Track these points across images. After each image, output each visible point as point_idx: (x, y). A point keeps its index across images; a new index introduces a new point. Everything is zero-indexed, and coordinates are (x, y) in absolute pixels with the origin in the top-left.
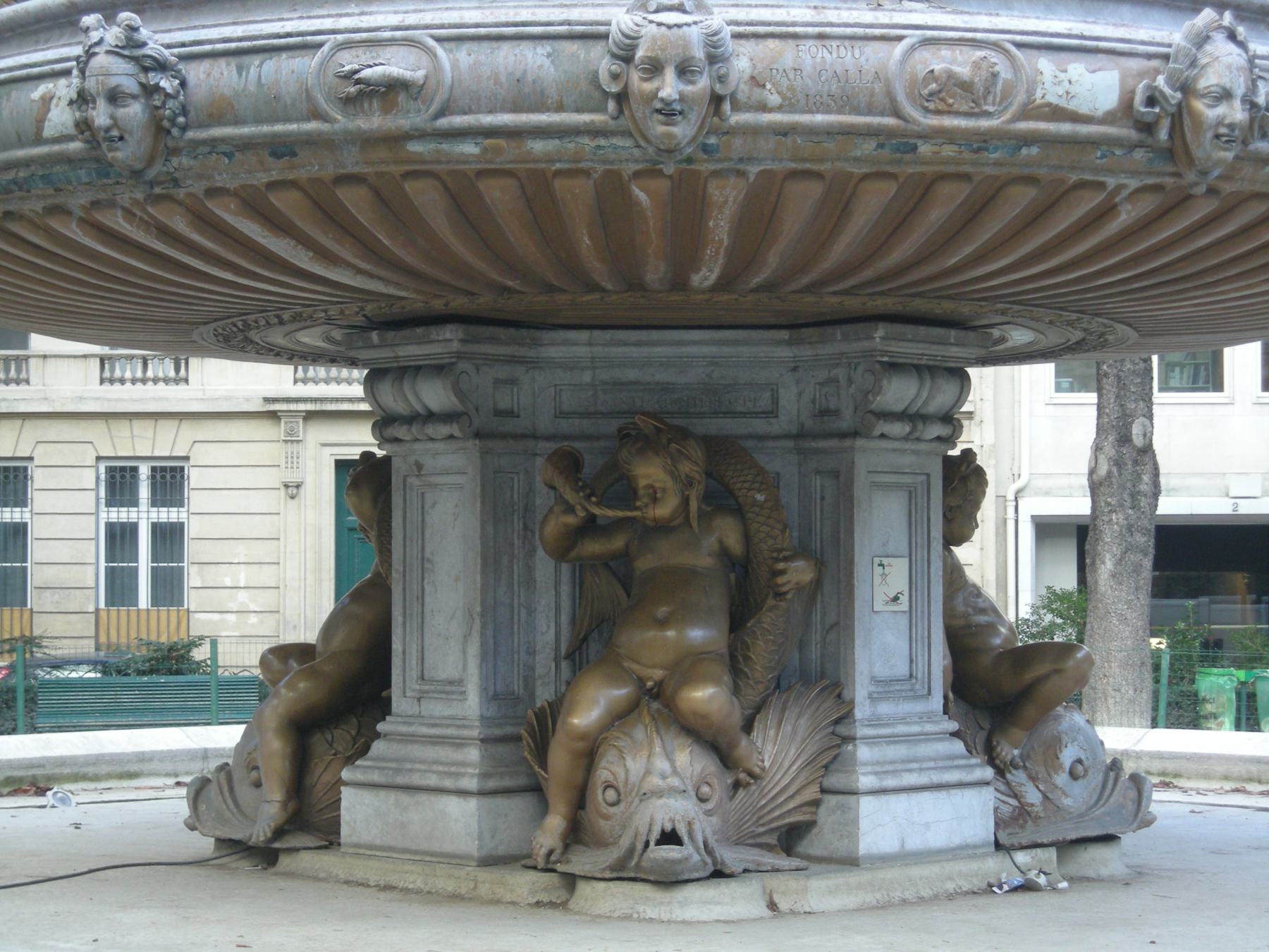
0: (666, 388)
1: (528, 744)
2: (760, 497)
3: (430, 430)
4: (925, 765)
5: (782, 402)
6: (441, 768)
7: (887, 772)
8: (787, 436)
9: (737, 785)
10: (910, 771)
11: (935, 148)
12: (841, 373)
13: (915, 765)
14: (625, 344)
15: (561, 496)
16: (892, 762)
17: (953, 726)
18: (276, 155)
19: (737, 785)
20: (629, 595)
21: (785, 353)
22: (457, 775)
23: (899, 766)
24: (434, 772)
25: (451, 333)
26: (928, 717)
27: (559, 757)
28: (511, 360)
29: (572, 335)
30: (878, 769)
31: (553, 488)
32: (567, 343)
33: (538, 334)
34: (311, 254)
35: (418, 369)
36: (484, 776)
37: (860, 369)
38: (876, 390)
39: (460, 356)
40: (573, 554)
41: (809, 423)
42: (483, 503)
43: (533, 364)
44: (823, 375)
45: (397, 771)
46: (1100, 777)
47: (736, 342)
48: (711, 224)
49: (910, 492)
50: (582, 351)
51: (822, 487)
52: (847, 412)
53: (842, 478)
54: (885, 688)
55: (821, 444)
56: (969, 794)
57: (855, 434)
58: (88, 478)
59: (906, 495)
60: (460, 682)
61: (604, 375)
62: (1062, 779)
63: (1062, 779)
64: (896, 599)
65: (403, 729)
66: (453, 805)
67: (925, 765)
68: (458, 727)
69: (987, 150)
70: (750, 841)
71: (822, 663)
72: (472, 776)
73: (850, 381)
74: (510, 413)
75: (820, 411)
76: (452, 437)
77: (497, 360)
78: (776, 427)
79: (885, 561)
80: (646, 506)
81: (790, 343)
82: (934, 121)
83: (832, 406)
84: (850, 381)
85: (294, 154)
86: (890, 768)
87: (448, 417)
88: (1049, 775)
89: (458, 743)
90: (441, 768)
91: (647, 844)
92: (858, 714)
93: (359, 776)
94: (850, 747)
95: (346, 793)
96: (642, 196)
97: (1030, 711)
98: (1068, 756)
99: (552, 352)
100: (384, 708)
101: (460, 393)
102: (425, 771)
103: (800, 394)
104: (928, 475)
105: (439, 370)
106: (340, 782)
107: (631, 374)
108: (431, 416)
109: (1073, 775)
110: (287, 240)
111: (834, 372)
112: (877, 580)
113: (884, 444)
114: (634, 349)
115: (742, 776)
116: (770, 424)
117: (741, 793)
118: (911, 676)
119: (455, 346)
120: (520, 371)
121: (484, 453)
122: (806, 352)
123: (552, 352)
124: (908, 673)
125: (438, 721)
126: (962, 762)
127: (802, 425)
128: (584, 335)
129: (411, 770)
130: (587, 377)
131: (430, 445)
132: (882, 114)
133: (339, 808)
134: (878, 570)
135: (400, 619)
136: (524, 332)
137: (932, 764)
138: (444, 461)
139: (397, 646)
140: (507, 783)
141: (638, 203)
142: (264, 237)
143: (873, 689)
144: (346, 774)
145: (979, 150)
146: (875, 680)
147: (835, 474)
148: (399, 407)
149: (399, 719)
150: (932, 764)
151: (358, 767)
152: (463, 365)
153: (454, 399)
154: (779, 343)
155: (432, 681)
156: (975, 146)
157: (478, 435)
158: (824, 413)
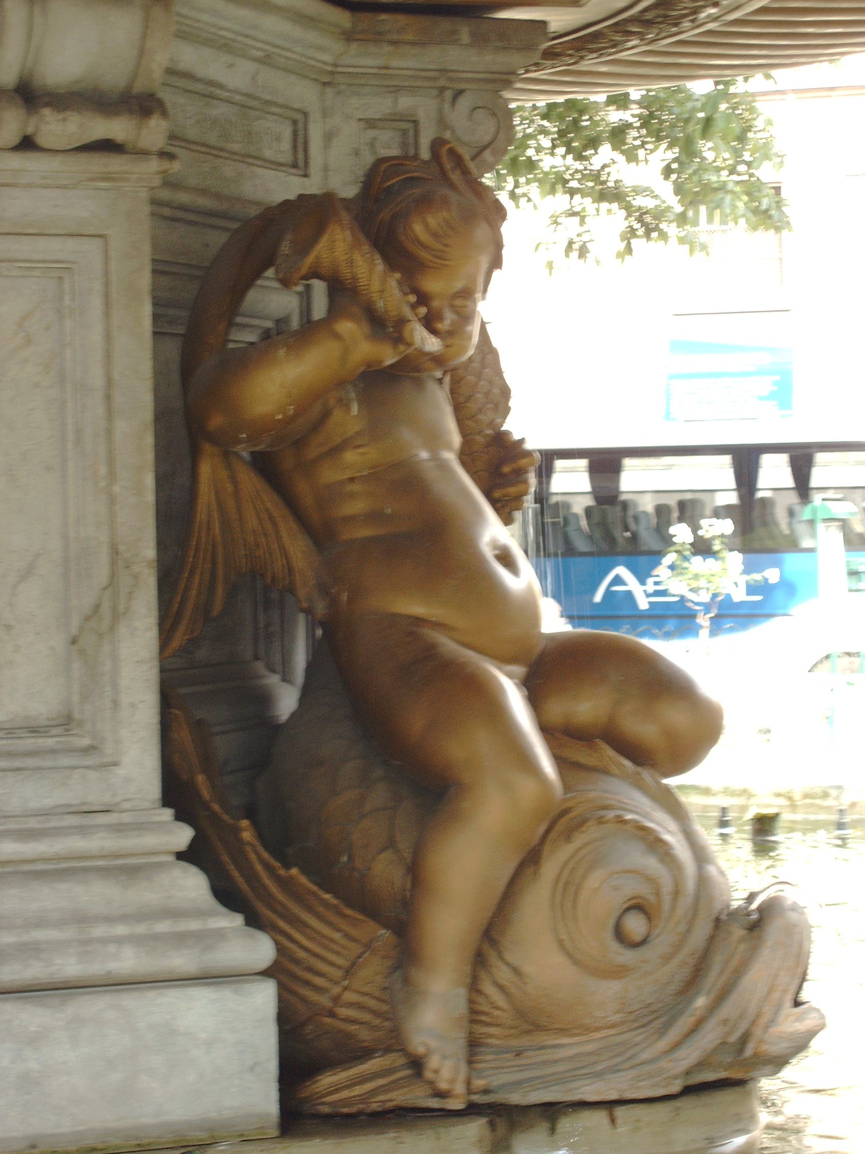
3: (56, 128)
27: (466, 863)
37: (464, 103)
44: (380, 106)
66: (197, 1009)
81: (349, 36)
89: (128, 870)
111: (405, 102)
122: (365, 59)
125: (32, 823)
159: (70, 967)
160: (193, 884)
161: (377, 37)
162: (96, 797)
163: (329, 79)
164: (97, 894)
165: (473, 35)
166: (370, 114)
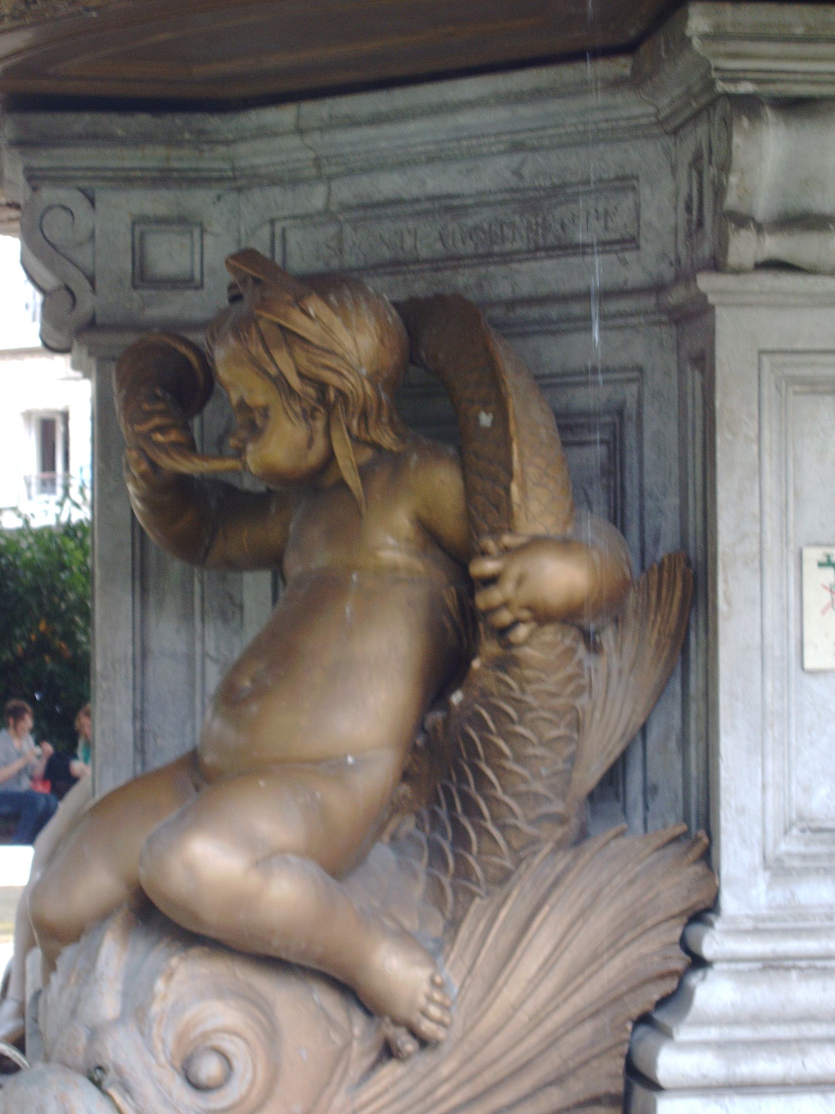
0: (447, 206)
14: (353, 123)
21: (632, 107)
28: (163, 178)
29: (271, 116)
33: (214, 123)
43: (239, 181)
47: (538, 95)
61: (346, 191)
81: (635, 81)
99: (255, 155)
107: (389, 184)
114: (370, 132)
116: (624, 263)
120: (199, 200)
136: (179, 120)
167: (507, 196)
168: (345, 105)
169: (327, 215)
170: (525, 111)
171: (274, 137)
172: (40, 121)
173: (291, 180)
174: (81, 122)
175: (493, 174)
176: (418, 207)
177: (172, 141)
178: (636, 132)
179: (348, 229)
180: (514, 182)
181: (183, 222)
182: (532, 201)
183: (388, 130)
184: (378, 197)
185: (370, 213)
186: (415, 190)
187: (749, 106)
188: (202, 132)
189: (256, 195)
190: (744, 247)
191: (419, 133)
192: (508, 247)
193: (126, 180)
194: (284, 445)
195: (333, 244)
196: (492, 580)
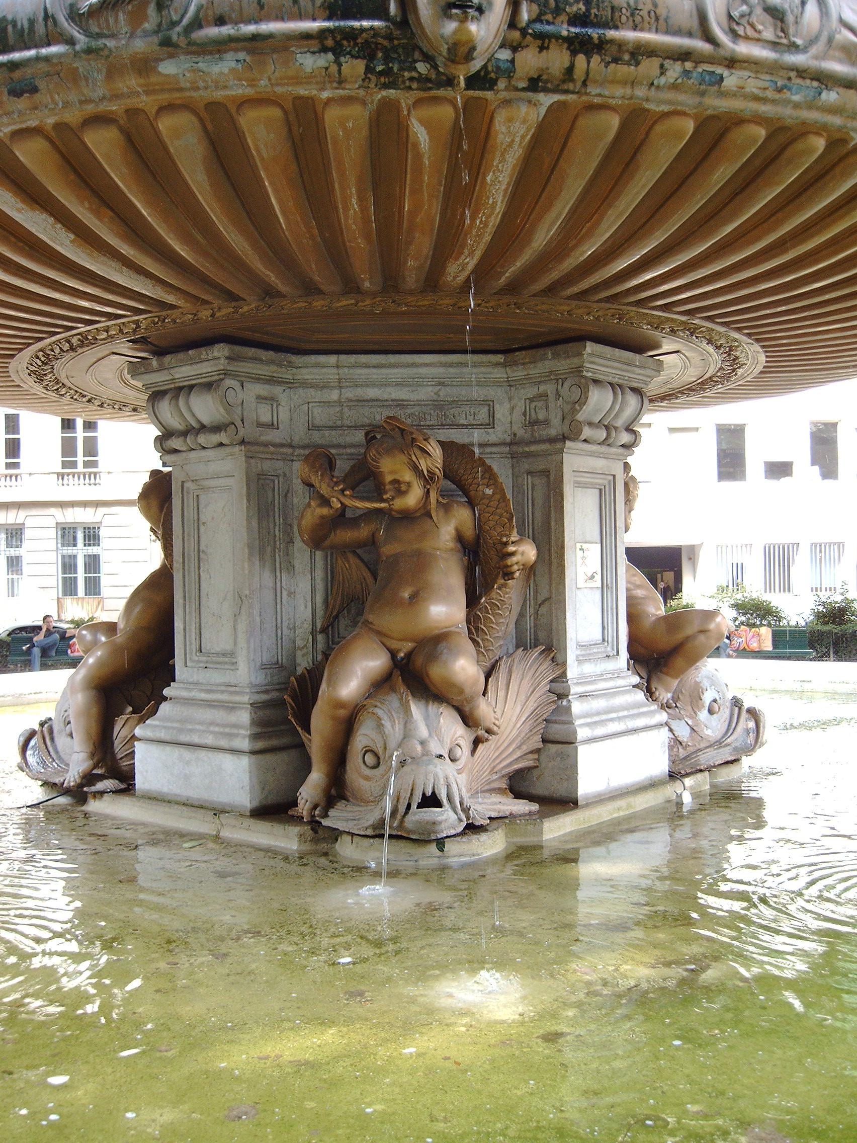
0: (400, 404)
1: (292, 708)
2: (489, 492)
3: (202, 439)
4: (621, 714)
5: (497, 416)
6: (217, 729)
7: (595, 723)
8: (504, 444)
9: (477, 742)
10: (612, 720)
11: (741, 83)
12: (549, 388)
13: (614, 715)
14: (367, 366)
15: (318, 492)
16: (598, 713)
17: (636, 680)
18: (16, 93)
19: (477, 742)
20: (375, 576)
21: (499, 374)
22: (231, 736)
23: (604, 717)
24: (212, 732)
25: (220, 351)
26: (616, 675)
27: (321, 722)
28: (271, 381)
29: (322, 359)
30: (589, 720)
31: (310, 485)
32: (317, 365)
33: (294, 358)
34: (72, 236)
35: (191, 387)
36: (255, 737)
37: (567, 385)
38: (582, 401)
39: (226, 374)
40: (327, 543)
41: (521, 433)
42: (248, 501)
43: (290, 385)
44: (531, 392)
45: (180, 730)
46: (728, 711)
48: (488, 178)
49: (600, 490)
50: (331, 374)
51: (533, 486)
52: (556, 421)
53: (552, 477)
54: (588, 652)
55: (533, 448)
56: (654, 733)
57: (564, 438)
58: (52, 533)
59: (597, 491)
60: (232, 654)
61: (349, 394)
62: (703, 715)
63: (703, 715)
64: (592, 577)
65: (185, 694)
67: (621, 714)
68: (231, 693)
69: (790, 89)
70: (487, 787)
71: (535, 632)
72: (244, 737)
73: (558, 395)
74: (271, 426)
75: (530, 422)
76: (221, 445)
77: (259, 379)
78: (493, 436)
79: (585, 546)
80: (393, 498)
81: (504, 365)
82: (743, 49)
83: (541, 416)
84: (558, 395)
85: (34, 90)
86: (596, 719)
87: (217, 429)
88: (695, 713)
89: (231, 707)
90: (217, 729)
91: (409, 807)
92: (570, 675)
93: (149, 734)
94: (565, 703)
95: (139, 747)
96: (420, 134)
97: (679, 661)
98: (708, 697)
99: (306, 374)
100: (169, 677)
101: (228, 406)
102: (204, 731)
103: (513, 409)
104: (614, 476)
105: (208, 386)
106: (134, 738)
107: (372, 393)
108: (202, 428)
109: (711, 712)
110: (44, 216)
111: (542, 388)
112: (579, 561)
113: (585, 446)
114: (374, 371)
115: (481, 733)
117: (481, 747)
118: (604, 640)
119: (222, 364)
120: (277, 390)
121: (249, 457)
122: (519, 373)
123: (306, 374)
124: (601, 638)
125: (214, 688)
126: (645, 709)
127: (515, 435)
128: (332, 359)
129: (191, 730)
130: (334, 395)
131: (203, 453)
132: (690, 34)
133: (134, 758)
134: (579, 554)
135: (181, 601)
136: (282, 356)
137: (625, 713)
138: (214, 467)
139: (178, 625)
140: (274, 742)
141: (416, 145)
142: (19, 211)
143: (579, 652)
144: (138, 731)
145: (780, 90)
146: (580, 646)
147: (546, 473)
148: (176, 423)
149: (182, 685)
150: (625, 713)
151: (149, 725)
152: (228, 382)
153: (222, 410)
154: (497, 364)
155: (208, 654)
156: (779, 84)
157: (243, 442)
158: (534, 423)
159: (196, 739)
160: (244, 717)
161: (515, 363)
162: (233, 681)
163: (510, 384)
164: (219, 715)
165: (553, 354)
166: (530, 395)
167: (430, 403)
168: (363, 358)
169: (339, 402)
170: (451, 370)
171: (325, 367)
172: (238, 349)
173: (324, 386)
174: (251, 352)
175: (426, 393)
176: (387, 403)
177: (280, 365)
178: (496, 383)
179: (346, 410)
180: (435, 397)
181: (271, 400)
182: (438, 405)
183: (384, 371)
184: (366, 397)
185: (361, 404)
186: (386, 397)
187: (596, 382)
188: (290, 362)
189: (301, 391)
190: (587, 432)
191: (375, 374)
192: (428, 423)
193: (258, 379)
194: (413, 499)
195: (338, 415)
196: (513, 554)
